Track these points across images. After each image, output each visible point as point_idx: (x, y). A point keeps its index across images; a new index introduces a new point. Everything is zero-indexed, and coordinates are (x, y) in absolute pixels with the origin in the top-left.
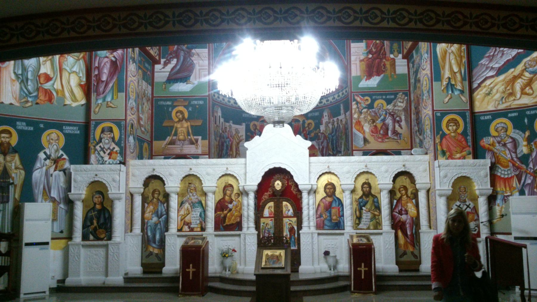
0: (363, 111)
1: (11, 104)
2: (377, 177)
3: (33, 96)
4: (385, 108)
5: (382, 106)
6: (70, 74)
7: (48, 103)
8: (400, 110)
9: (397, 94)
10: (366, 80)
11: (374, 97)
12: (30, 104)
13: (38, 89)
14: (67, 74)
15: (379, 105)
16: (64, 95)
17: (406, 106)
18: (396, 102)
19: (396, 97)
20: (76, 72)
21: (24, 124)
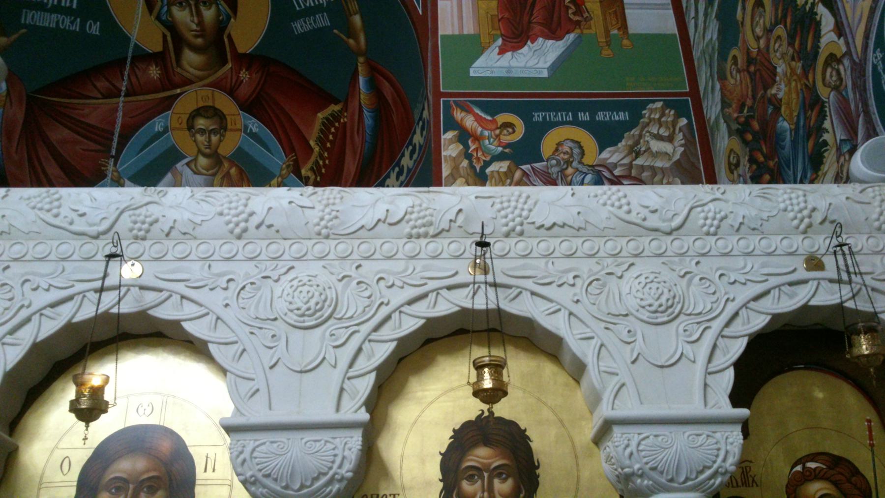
0: (488, 171)
2: (590, 359)
4: (589, 159)
5: (576, 151)
8: (662, 169)
9: (643, 105)
10: (502, 52)
11: (538, 117)
15: (566, 148)
17: (684, 154)
18: (641, 136)
19: (635, 120)
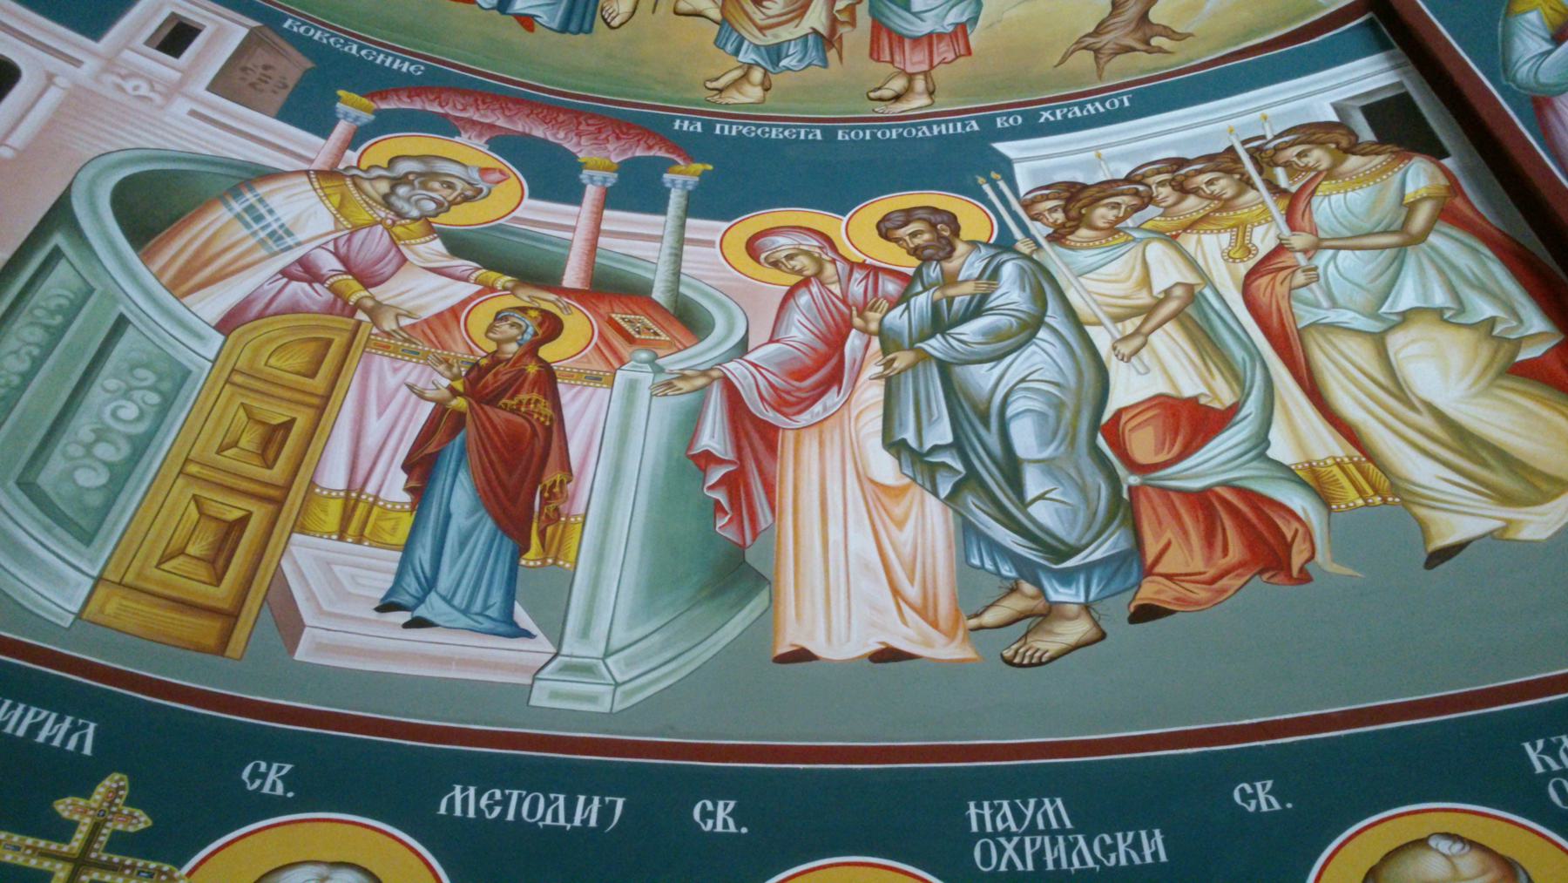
1: (889, 655)
3: (1089, 568)
6: (1379, 342)
7: (1263, 589)
12: (1075, 630)
13: (1125, 510)
14: (1362, 353)
16: (1397, 490)
20: (1439, 312)
21: (1054, 809)
